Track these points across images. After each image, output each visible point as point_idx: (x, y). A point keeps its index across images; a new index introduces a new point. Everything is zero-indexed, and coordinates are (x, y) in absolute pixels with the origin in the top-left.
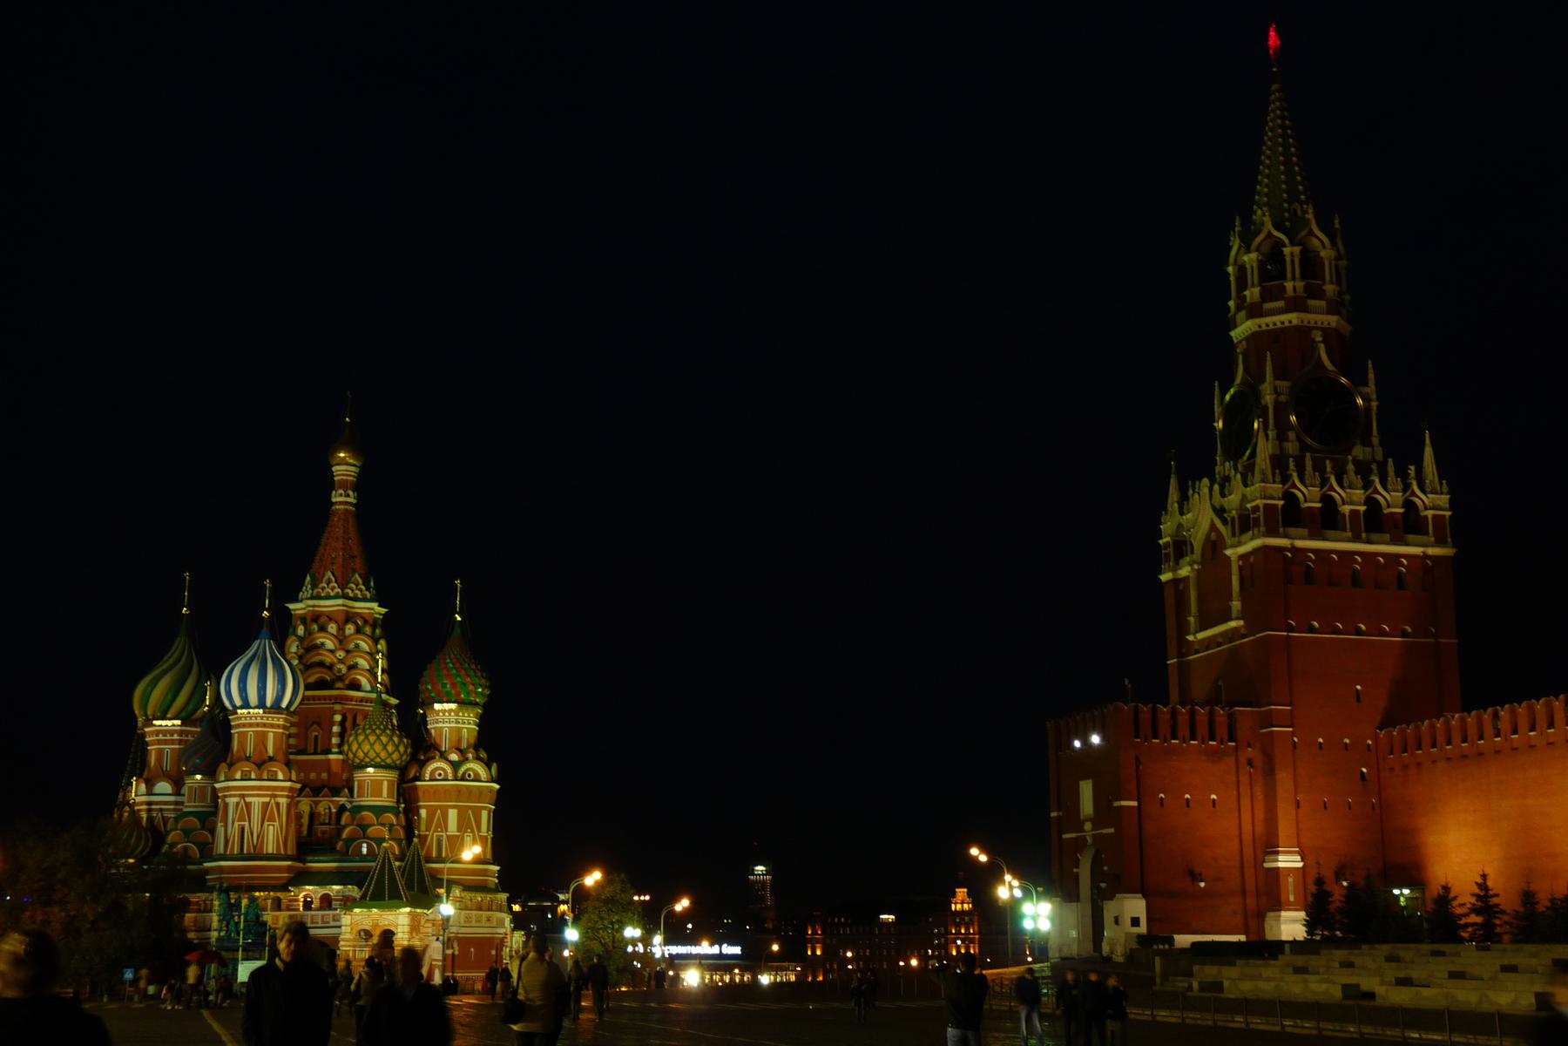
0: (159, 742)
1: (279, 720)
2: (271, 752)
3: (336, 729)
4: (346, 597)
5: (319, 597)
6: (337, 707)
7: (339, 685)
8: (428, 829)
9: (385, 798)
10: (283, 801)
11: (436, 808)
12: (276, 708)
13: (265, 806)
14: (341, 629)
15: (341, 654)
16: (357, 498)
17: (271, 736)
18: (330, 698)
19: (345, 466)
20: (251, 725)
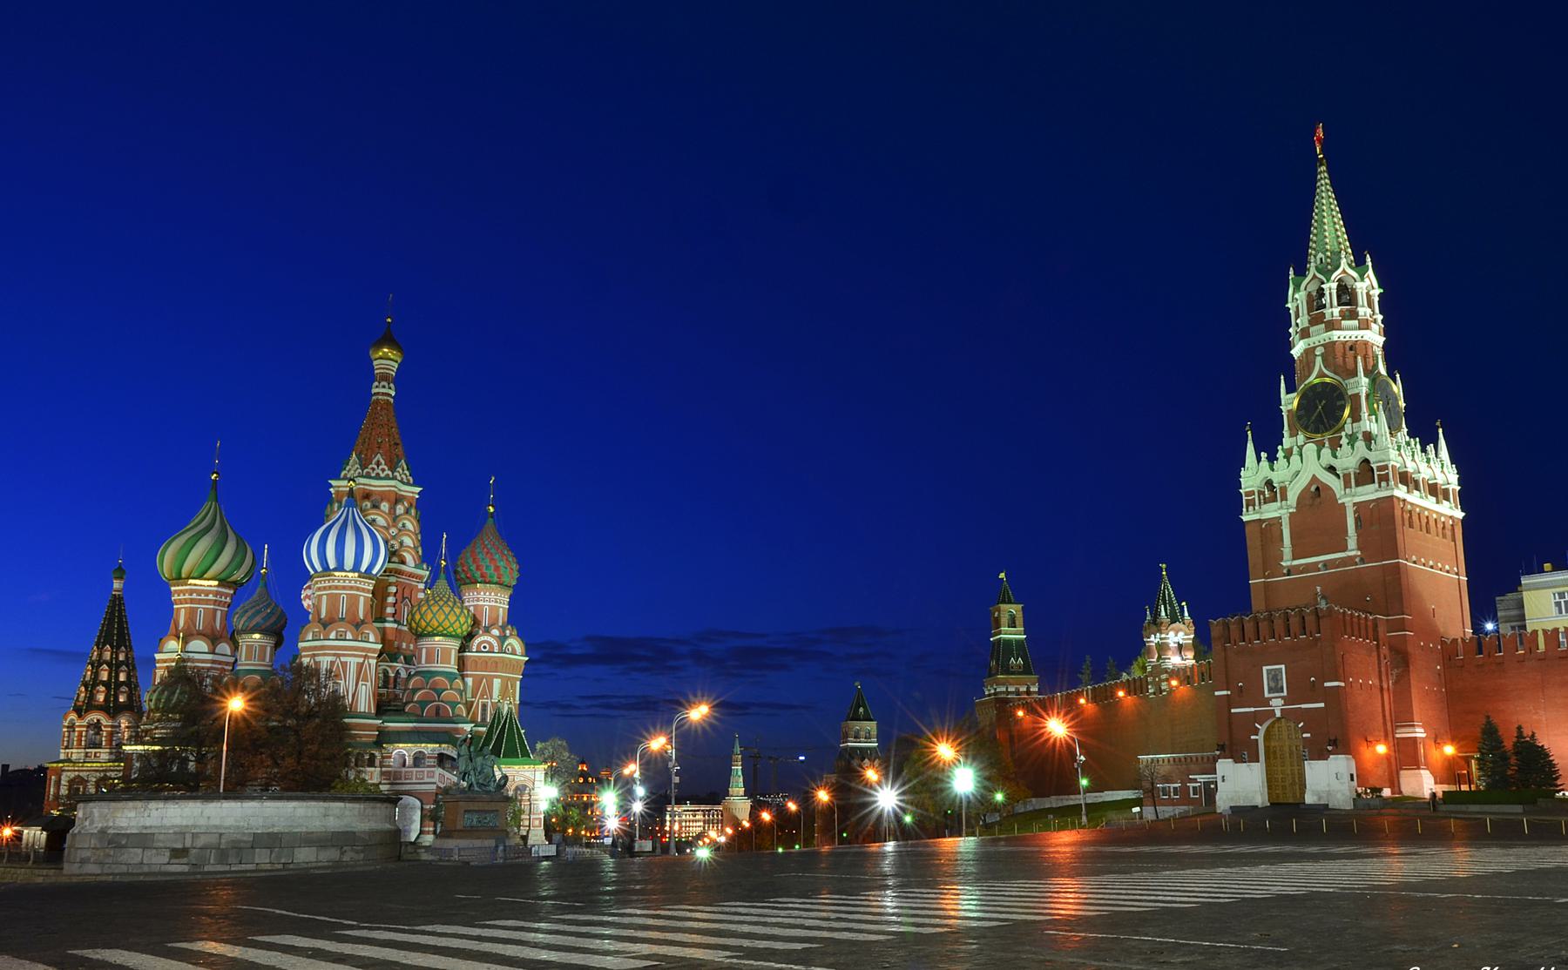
2: (361, 616)
3: (391, 600)
4: (394, 478)
6: (392, 579)
8: (474, 696)
9: (452, 667)
13: (360, 666)
14: (393, 509)
15: (393, 531)
19: (387, 360)
20: (344, 588)
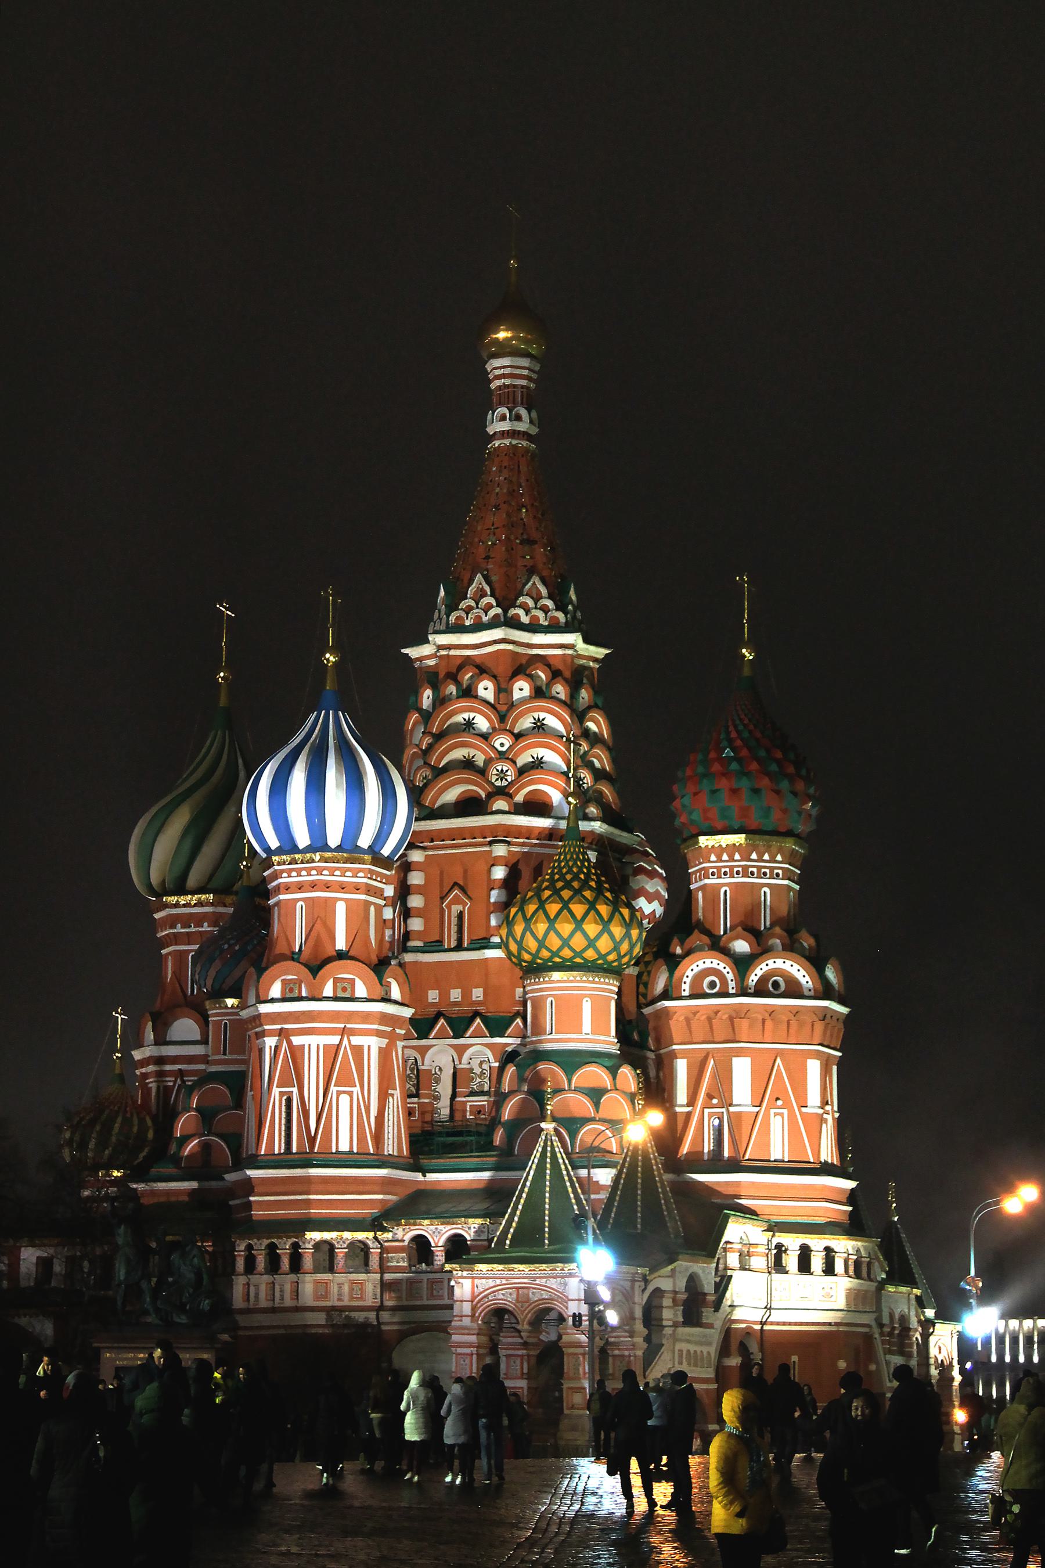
0: (176, 939)
1: (359, 874)
4: (514, 624)
5: (459, 628)
6: (500, 850)
7: (501, 804)
10: (373, 1044)
11: (707, 1055)
12: (349, 850)
13: (332, 1053)
16: (540, 422)
17: (341, 909)
18: (483, 832)
